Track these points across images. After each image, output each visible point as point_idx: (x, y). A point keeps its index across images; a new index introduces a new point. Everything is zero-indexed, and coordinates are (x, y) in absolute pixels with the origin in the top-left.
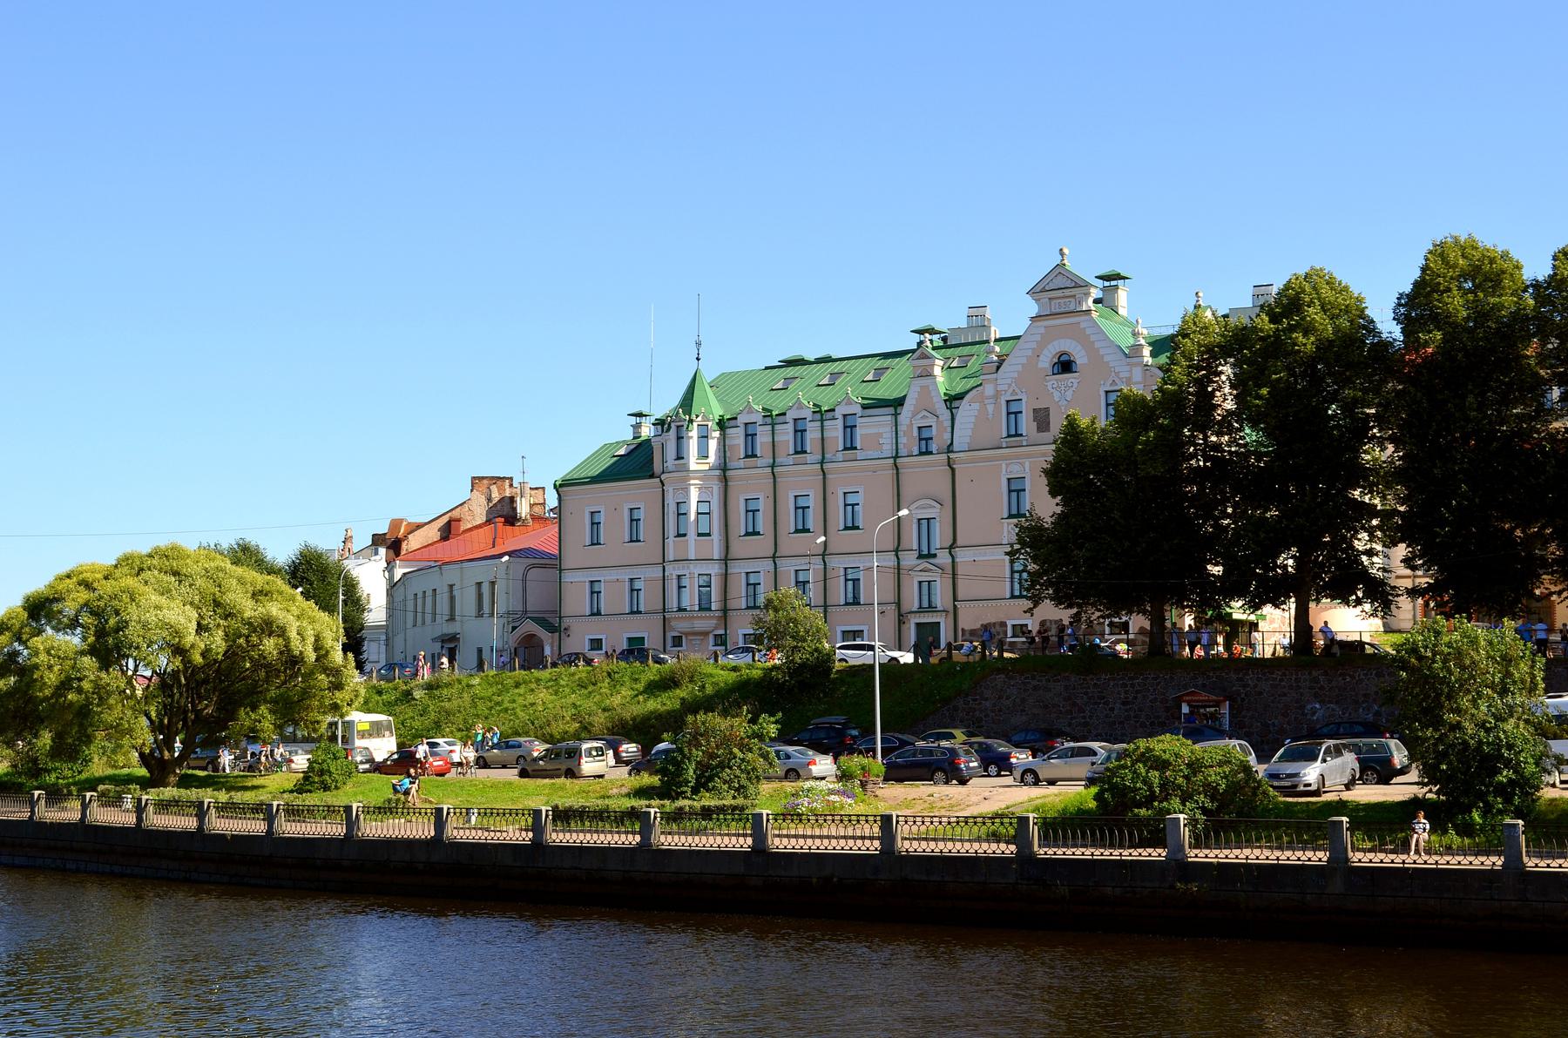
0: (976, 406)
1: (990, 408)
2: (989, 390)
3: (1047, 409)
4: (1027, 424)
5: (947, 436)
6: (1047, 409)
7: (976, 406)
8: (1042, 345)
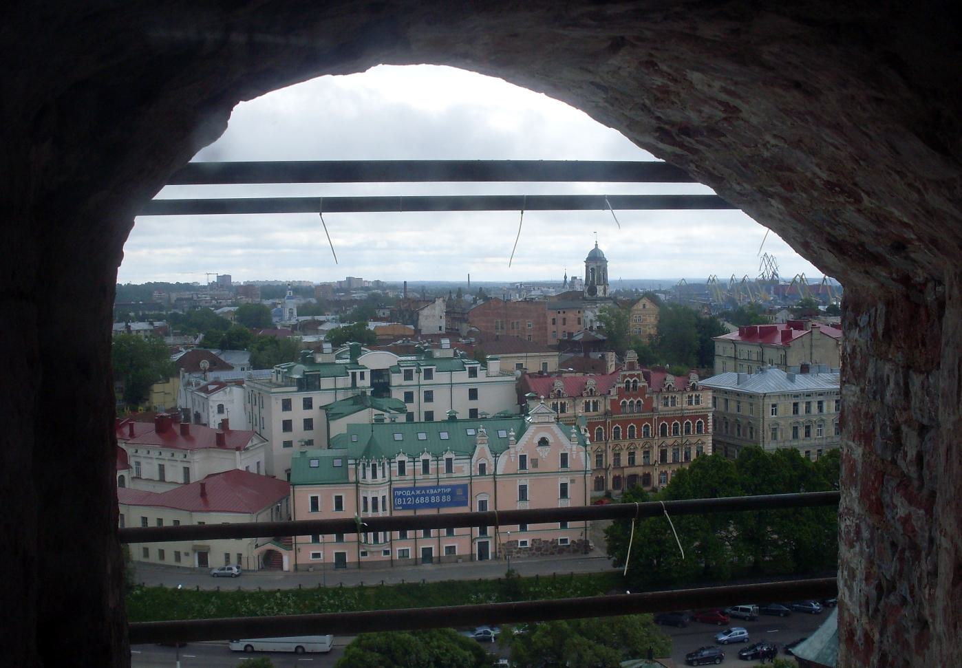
0: (507, 456)
2: (512, 451)
3: (537, 459)
5: (493, 468)
7: (507, 456)
8: (535, 433)
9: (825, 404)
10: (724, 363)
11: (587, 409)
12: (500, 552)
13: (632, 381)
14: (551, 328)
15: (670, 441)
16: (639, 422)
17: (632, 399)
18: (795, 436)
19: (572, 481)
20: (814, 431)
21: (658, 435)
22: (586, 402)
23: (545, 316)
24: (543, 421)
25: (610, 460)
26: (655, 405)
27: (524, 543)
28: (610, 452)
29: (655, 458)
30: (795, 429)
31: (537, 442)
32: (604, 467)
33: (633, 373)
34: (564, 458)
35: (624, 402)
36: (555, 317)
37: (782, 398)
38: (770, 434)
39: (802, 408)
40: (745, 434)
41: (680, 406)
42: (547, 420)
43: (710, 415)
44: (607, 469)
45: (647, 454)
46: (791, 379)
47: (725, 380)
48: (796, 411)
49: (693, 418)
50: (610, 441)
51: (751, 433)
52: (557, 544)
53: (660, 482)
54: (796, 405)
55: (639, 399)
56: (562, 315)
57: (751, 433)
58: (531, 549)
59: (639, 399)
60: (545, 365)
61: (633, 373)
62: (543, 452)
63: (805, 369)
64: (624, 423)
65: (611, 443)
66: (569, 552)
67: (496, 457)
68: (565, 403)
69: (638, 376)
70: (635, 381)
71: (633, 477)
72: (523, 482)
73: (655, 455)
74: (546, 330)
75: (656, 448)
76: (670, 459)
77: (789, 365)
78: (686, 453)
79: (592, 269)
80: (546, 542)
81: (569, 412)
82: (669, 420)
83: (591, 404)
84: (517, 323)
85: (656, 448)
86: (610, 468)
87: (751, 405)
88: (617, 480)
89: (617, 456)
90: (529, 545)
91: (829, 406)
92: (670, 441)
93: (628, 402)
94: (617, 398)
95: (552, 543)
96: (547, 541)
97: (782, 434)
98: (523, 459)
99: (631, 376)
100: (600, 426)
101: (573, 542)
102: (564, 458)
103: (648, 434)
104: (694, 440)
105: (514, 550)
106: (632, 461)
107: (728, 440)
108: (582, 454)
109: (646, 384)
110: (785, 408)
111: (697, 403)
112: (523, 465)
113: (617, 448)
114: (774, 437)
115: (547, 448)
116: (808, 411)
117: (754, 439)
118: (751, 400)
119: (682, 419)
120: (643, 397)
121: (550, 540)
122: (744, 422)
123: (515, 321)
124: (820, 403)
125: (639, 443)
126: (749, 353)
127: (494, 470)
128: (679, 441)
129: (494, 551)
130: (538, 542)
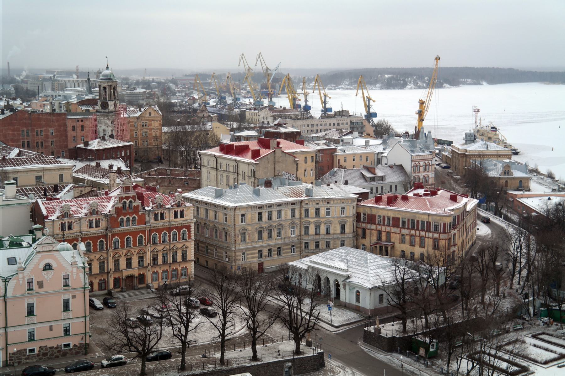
0: (15, 281)
1: (21, 282)
2: (21, 276)
3: (42, 282)
4: (35, 286)
6: (42, 282)
7: (15, 281)
9: (283, 213)
10: (208, 172)
11: (91, 227)
12: (10, 360)
13: (128, 202)
14: (70, 133)
15: (160, 248)
16: (134, 233)
17: (128, 216)
18: (260, 237)
19: (74, 297)
20: (274, 234)
21: (150, 243)
22: (89, 220)
23: (65, 125)
24: (47, 250)
25: (111, 266)
26: (147, 219)
27: (32, 351)
28: (111, 260)
29: (148, 261)
30: (260, 233)
31: (42, 267)
32: (106, 271)
34: (66, 278)
35: (122, 219)
36: (75, 124)
37: (250, 209)
38: (240, 237)
39: (265, 216)
40: (221, 237)
41: (168, 219)
42: (51, 249)
43: (192, 225)
44: (108, 273)
45: (141, 259)
46: (257, 193)
47: (203, 195)
48: (260, 219)
49: (179, 228)
50: (110, 250)
51: (226, 236)
52: (61, 348)
53: (152, 280)
54: (260, 214)
55: (134, 215)
56: (81, 123)
57: (226, 236)
58: (38, 355)
59: (134, 215)
60: (61, 177)
62: (47, 276)
63: (268, 184)
64: (122, 235)
65: (111, 252)
66: (72, 354)
67: (6, 282)
68: (72, 222)
69: (133, 197)
70: (131, 202)
71: (131, 277)
72: (31, 301)
73: (148, 259)
74: (66, 137)
75: (148, 254)
76: (160, 260)
77: (257, 177)
78: (173, 256)
79: (105, 88)
80: (51, 348)
81: (76, 228)
82: (159, 231)
83: (94, 221)
84: (41, 131)
85: (148, 254)
86: (111, 272)
87: (226, 214)
88: (117, 281)
89: (117, 262)
90: (36, 352)
91: (286, 214)
92: (160, 248)
93: (125, 219)
94: (116, 216)
95: (57, 348)
96: (53, 347)
97: (249, 237)
98: (30, 283)
99: (127, 198)
101: (75, 346)
102: (66, 278)
103: (142, 243)
104: (179, 246)
105: (23, 358)
107: (208, 241)
108: (82, 275)
109: (140, 204)
110: (252, 216)
111: (182, 216)
112: (30, 289)
113: (117, 256)
114: (243, 240)
115: (51, 272)
116: (270, 218)
117: (228, 241)
118: (225, 211)
119: (170, 229)
120: (137, 214)
121: (55, 346)
122: (220, 227)
123: (39, 130)
124: (280, 212)
125: (135, 251)
126: (228, 166)
127: (4, 293)
128: (168, 247)
129: (5, 359)
130: (44, 348)
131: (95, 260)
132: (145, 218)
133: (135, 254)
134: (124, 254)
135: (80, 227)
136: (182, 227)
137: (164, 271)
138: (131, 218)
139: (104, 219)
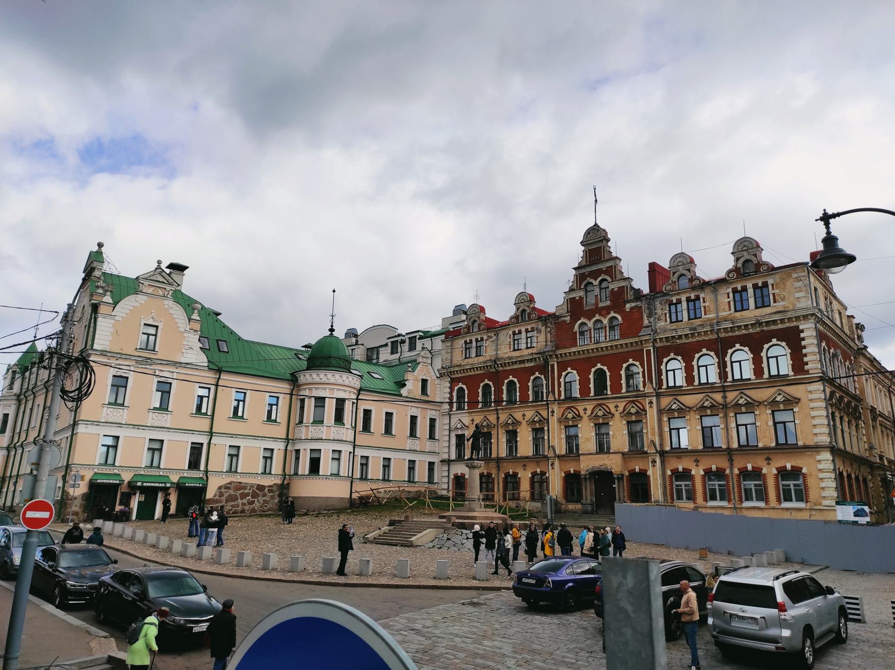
17: (597, 317)
33: (600, 267)
55: (612, 314)
61: (600, 267)
93: (590, 324)
100: (537, 374)
106: (603, 448)
131: (524, 423)
132: (642, 319)
133: (617, 415)
134: (589, 412)
135: (497, 350)
136: (766, 337)
137: (708, 473)
138: (605, 321)
139: (543, 329)
